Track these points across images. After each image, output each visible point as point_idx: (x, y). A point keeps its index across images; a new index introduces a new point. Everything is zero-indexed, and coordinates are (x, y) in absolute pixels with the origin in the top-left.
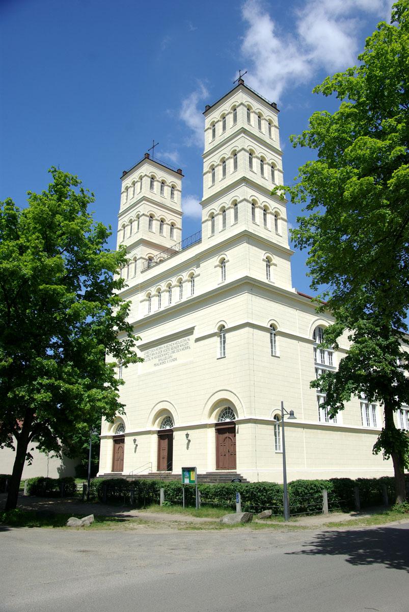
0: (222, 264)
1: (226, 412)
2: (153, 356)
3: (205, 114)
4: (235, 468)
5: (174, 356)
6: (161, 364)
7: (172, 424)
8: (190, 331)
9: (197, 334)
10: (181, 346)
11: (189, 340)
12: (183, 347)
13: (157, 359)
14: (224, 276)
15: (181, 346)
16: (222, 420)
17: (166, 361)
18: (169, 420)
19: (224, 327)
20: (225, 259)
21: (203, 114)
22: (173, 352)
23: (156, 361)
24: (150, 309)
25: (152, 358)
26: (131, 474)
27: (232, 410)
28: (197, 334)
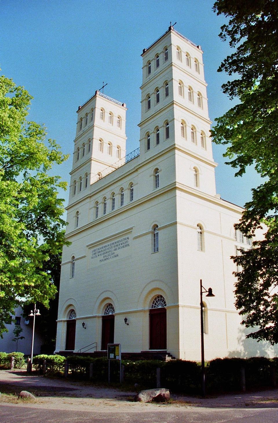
0: (156, 173)
1: (159, 300)
2: (99, 254)
3: (143, 55)
4: (165, 348)
5: (116, 252)
6: (105, 260)
7: (114, 310)
8: (129, 231)
9: (135, 233)
10: (121, 244)
11: (128, 238)
12: (123, 245)
13: (103, 256)
14: (157, 185)
15: (121, 244)
16: (155, 307)
17: (110, 257)
18: (110, 306)
19: (157, 226)
20: (158, 170)
21: (141, 55)
22: (115, 250)
23: (102, 257)
24: (97, 215)
25: (99, 255)
26: (79, 352)
27: (163, 298)
28: (135, 233)
